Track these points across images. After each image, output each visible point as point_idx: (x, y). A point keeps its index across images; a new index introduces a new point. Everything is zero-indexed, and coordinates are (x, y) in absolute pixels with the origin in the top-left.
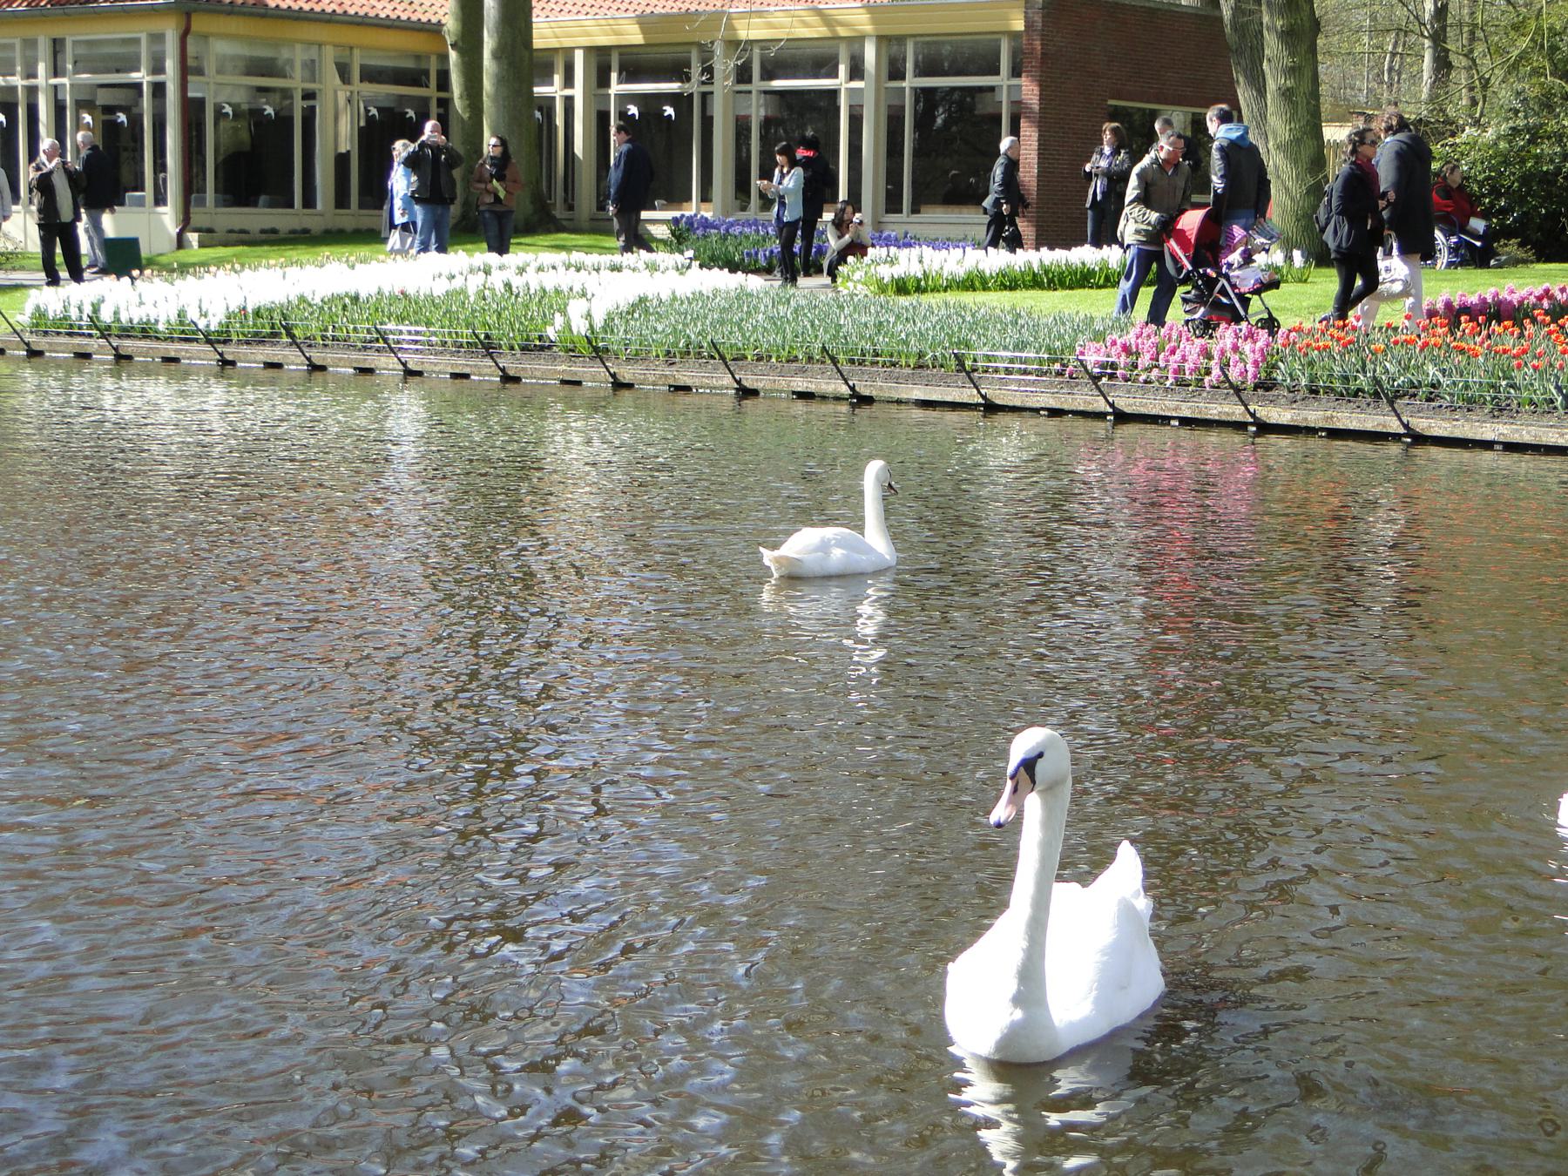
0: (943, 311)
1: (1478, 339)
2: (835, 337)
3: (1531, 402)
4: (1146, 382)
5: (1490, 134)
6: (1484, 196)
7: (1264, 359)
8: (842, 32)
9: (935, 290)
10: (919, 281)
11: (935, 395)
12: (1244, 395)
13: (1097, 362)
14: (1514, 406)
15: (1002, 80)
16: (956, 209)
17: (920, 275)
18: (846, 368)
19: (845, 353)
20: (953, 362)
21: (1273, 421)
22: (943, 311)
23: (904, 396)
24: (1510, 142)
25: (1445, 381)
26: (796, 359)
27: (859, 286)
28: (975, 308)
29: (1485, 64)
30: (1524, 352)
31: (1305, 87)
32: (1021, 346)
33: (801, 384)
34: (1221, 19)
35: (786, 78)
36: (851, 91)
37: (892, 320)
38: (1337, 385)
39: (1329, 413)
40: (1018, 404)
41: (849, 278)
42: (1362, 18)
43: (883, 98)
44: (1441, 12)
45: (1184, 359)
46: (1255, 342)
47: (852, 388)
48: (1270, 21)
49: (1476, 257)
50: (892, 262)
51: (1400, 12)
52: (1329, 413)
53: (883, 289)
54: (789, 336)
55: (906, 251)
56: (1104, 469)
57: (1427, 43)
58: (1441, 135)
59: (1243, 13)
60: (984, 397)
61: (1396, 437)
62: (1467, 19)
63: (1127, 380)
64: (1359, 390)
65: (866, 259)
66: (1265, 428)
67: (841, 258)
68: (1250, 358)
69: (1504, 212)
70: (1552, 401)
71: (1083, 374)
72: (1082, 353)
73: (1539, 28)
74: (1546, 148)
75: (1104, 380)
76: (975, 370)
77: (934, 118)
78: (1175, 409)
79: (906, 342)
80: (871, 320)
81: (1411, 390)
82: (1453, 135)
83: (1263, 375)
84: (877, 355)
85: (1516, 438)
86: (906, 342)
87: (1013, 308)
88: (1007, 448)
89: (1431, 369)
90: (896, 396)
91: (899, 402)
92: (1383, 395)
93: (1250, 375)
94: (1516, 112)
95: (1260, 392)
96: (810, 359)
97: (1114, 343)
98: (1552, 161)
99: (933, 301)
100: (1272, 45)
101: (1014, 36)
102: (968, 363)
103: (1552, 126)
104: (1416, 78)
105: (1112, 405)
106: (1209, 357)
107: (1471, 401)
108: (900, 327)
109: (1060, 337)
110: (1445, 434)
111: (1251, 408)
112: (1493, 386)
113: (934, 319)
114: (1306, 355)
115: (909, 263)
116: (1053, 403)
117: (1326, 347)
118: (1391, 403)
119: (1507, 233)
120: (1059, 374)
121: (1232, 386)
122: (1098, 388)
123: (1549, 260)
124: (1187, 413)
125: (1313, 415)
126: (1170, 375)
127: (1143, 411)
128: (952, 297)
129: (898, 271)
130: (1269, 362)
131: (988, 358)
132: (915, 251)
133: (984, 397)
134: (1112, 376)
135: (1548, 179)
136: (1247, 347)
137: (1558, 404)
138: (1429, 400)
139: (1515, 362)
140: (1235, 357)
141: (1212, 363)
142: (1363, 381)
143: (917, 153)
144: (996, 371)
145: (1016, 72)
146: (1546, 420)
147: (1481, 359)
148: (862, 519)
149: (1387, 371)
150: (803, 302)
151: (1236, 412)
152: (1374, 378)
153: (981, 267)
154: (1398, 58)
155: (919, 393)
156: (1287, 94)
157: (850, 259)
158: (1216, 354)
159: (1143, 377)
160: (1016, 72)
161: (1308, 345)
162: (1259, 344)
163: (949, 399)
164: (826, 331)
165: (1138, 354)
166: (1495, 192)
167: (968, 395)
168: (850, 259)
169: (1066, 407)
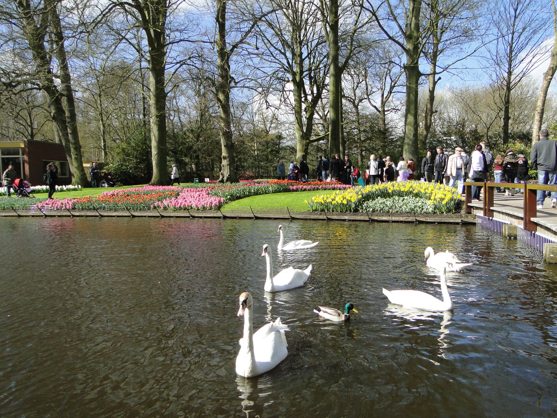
5: (115, 165)
31: (79, 157)
49: (112, 186)
66: (74, 216)
81: (100, 208)
119: (118, 181)
125: (83, 213)
130: (74, 204)
140: (67, 204)
142: (91, 207)
151: (68, 214)
156: (76, 158)
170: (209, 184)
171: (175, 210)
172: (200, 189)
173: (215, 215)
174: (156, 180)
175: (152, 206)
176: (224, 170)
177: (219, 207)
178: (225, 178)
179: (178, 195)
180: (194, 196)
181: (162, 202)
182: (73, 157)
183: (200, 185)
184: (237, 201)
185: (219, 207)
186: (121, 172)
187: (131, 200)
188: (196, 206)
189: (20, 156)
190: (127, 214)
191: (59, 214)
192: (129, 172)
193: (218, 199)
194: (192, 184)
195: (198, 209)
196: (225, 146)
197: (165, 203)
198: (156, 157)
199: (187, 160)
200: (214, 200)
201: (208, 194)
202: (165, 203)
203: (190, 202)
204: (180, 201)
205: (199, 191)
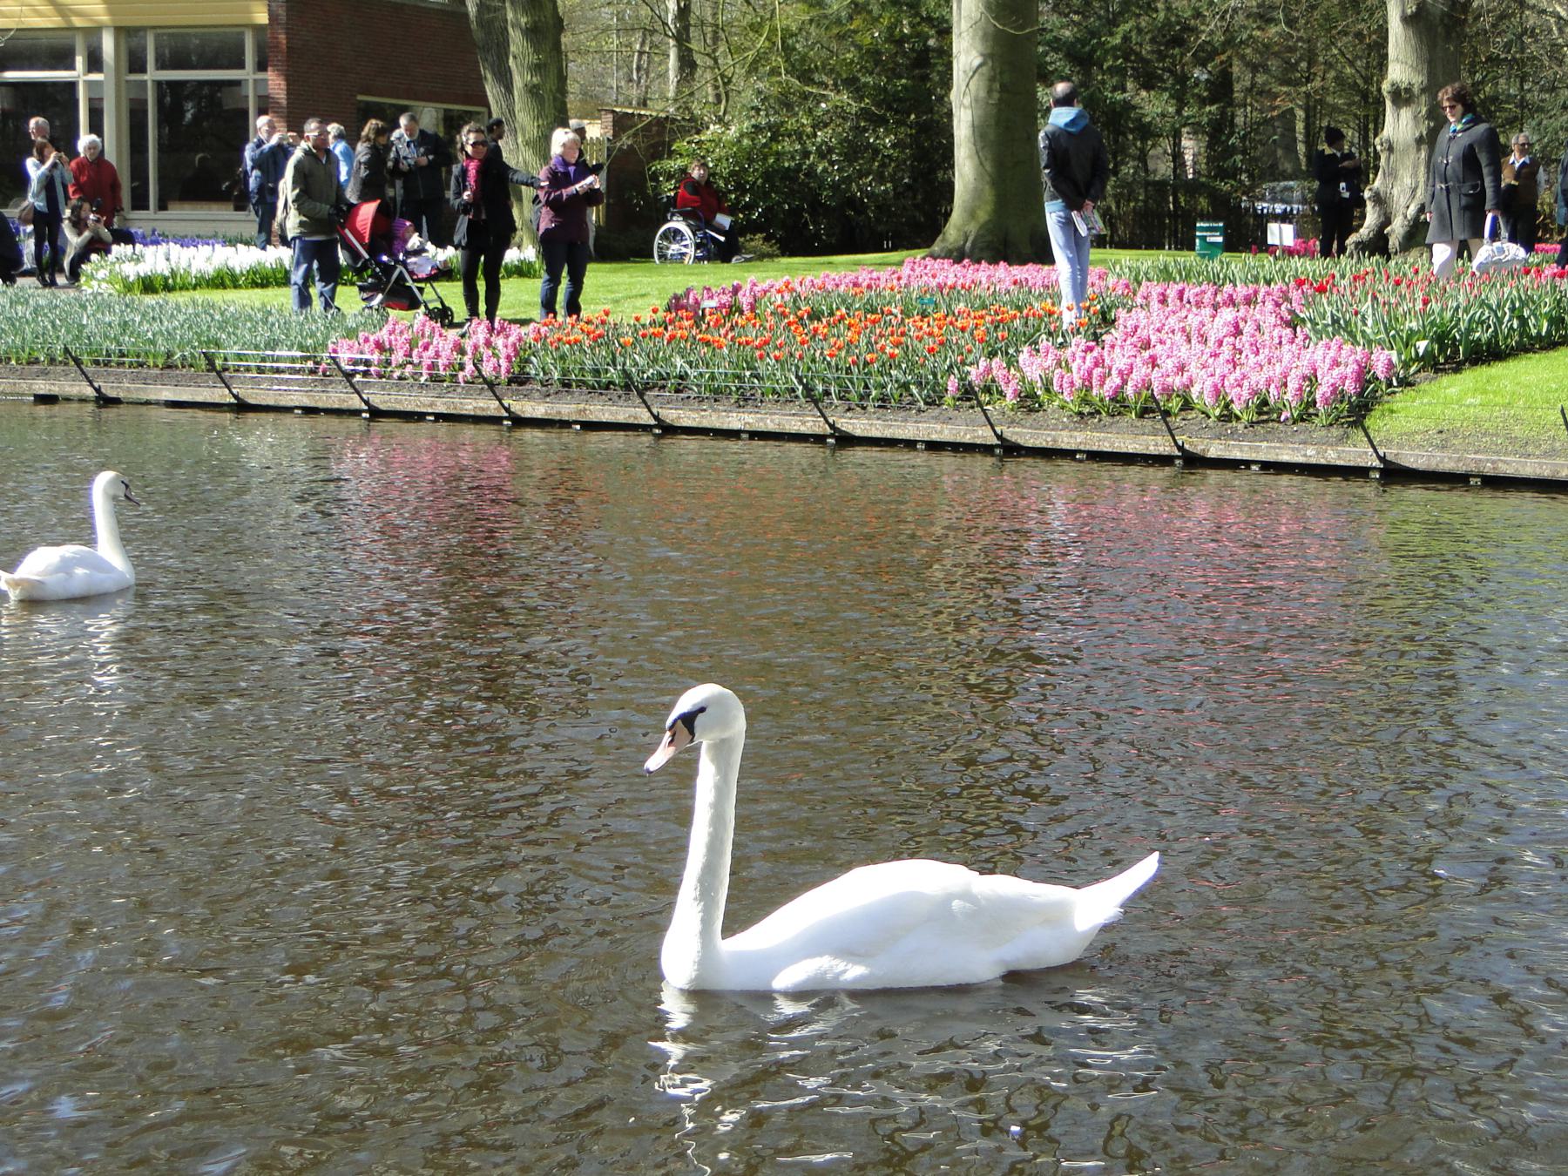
0: (191, 310)
1: (722, 331)
2: (78, 338)
3: (774, 392)
4: (400, 378)
5: (733, 131)
6: (730, 192)
7: (517, 354)
8: (78, 22)
9: (183, 288)
10: (166, 279)
11: (185, 395)
12: (498, 390)
13: (350, 359)
14: (758, 396)
15: (247, 74)
16: (205, 205)
17: (167, 273)
18: (91, 370)
19: (89, 354)
20: (203, 362)
21: (528, 415)
22: (191, 310)
23: (153, 397)
24: (753, 140)
25: (692, 373)
26: (37, 361)
27: (104, 285)
28: (224, 307)
29: (726, 62)
30: (766, 343)
31: (551, 84)
32: (273, 344)
33: (42, 387)
34: (466, 15)
35: (21, 68)
36: (89, 84)
37: (138, 319)
38: (589, 378)
39: (581, 406)
40: (271, 403)
41: (92, 277)
42: (607, 15)
43: (123, 94)
44: (683, 13)
45: (437, 355)
46: (507, 337)
47: (98, 390)
48: (515, 19)
49: (720, 251)
50: (138, 259)
51: (645, 11)
52: (581, 406)
53: (128, 288)
54: (29, 337)
55: (152, 248)
56: (359, 461)
57: (672, 42)
58: (684, 132)
59: (489, 9)
60: (236, 397)
61: (646, 428)
62: (710, 19)
63: (380, 376)
64: (611, 383)
65: (111, 257)
66: (520, 422)
67: (82, 257)
68: (503, 352)
69: (750, 207)
70: (793, 390)
71: (337, 372)
72: (335, 351)
73: (773, 30)
74: (786, 145)
75: (358, 378)
76: (226, 369)
77: (183, 113)
78: (431, 405)
79: (153, 342)
80: (116, 320)
81: (659, 382)
82: (698, 132)
83: (517, 370)
84: (123, 355)
85: (761, 427)
86: (153, 342)
87: (264, 305)
88: (259, 443)
89: (679, 361)
90: (144, 397)
91: (148, 403)
92: (631, 387)
93: (503, 370)
94: (758, 110)
95: (514, 386)
96: (52, 361)
97: (367, 340)
98: (793, 158)
99: (181, 300)
100: (517, 42)
101: (258, 29)
102: (218, 363)
103: (791, 124)
104: (663, 76)
105: (367, 403)
106: (462, 352)
107: (717, 391)
108: (146, 326)
109: (313, 335)
110: (694, 424)
111: (506, 403)
112: (738, 377)
113: (181, 318)
114: (557, 349)
115: (155, 260)
116: (306, 402)
117: (576, 341)
118: (641, 395)
119: (754, 228)
120: (313, 372)
121: (485, 381)
122: (352, 386)
123: (793, 254)
124: (442, 409)
125: (566, 408)
126: (425, 372)
127: (399, 407)
128: (200, 295)
129: (144, 269)
130: (521, 355)
131: (239, 357)
132: (163, 248)
133: (236, 397)
134: (366, 374)
135: (789, 175)
136: (499, 342)
137: (799, 393)
138: (677, 391)
139: (757, 353)
140: (486, 353)
141: (466, 359)
142: (613, 374)
143: (161, 148)
144: (248, 369)
145: (262, 66)
146: (788, 409)
147: (725, 351)
148: (93, 528)
149: (636, 364)
150: (42, 302)
151: (490, 406)
152: (624, 371)
153: (230, 264)
154: (645, 57)
155: (168, 394)
156: (532, 91)
157: (94, 257)
158: (469, 350)
159: (397, 374)
160: (262, 66)
161: (559, 340)
162: (512, 339)
163: (200, 399)
164: (68, 332)
165: (391, 351)
166: (741, 189)
167: (220, 395)
168: (94, 257)
169: (320, 405)
170: (1296, 262)
171: (1088, 413)
172: (1241, 291)
173: (1332, 457)
174: (973, 229)
175: (952, 383)
176: (1392, 174)
177: (1358, 408)
178: (1397, 229)
179: (1107, 321)
180: (1208, 332)
181: (1012, 362)
182: (518, 83)
183: (1239, 263)
184: (1471, 377)
185: (1358, 408)
186: (767, 176)
187: (831, 345)
188: (1217, 392)
189: (247, 74)
190: (810, 423)
191: (441, 408)
192: (811, 172)
193: (1351, 357)
194: (1188, 258)
195: (1228, 416)
196: (1407, 20)
197: (1032, 366)
198: (978, 86)
199: (1153, 105)
200: (1331, 364)
201: (1288, 324)
202: (1032, 366)
203: (1181, 368)
204: (1119, 360)
205: (1231, 301)
